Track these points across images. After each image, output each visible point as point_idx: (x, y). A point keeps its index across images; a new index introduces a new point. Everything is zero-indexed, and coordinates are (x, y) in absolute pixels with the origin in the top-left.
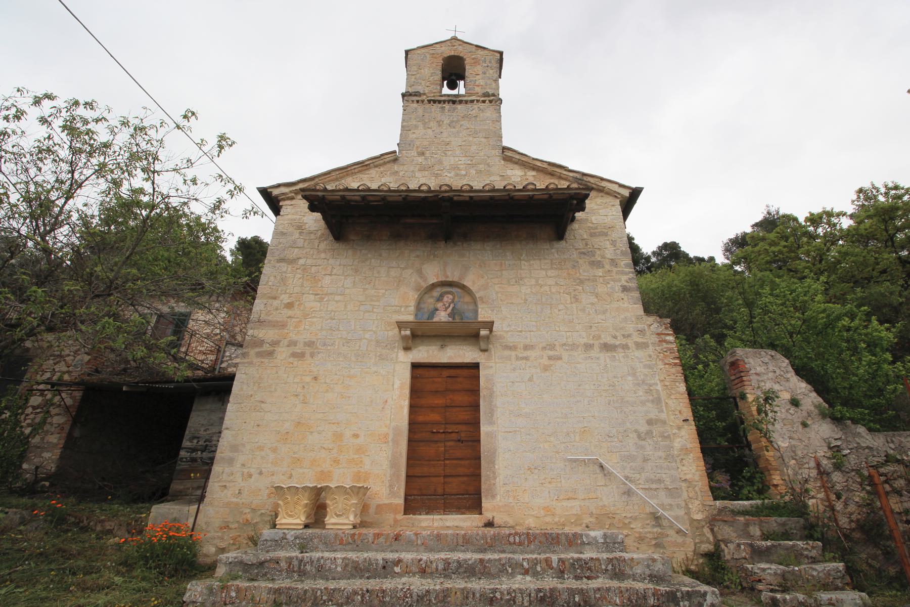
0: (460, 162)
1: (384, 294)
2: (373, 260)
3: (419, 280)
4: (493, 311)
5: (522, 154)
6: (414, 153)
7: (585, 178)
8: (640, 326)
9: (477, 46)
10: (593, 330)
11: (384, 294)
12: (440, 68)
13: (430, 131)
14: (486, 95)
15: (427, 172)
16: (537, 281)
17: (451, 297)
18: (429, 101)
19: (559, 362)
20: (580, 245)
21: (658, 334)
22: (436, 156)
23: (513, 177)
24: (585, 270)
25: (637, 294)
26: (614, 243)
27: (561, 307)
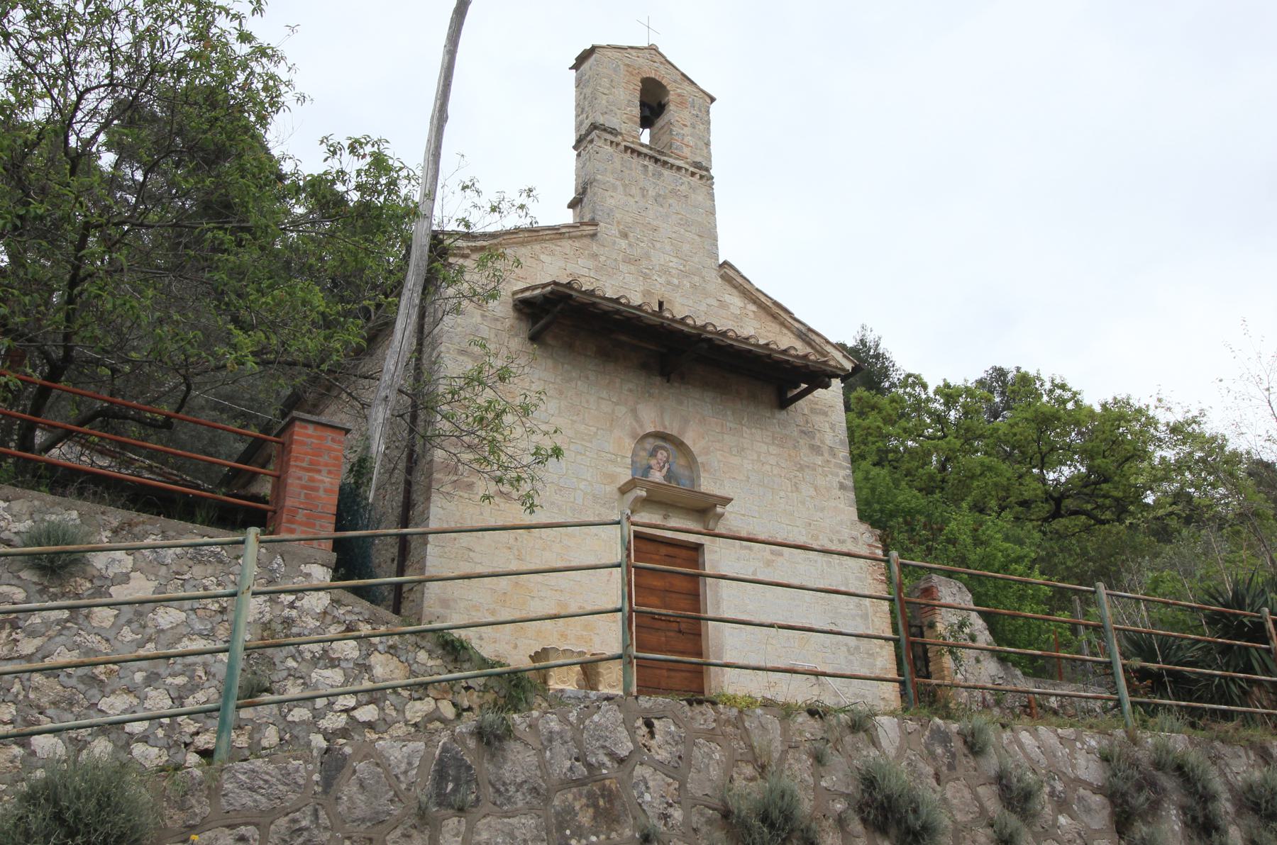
0: (671, 264)
1: (596, 433)
2: (579, 383)
3: (634, 423)
4: (715, 483)
5: (745, 278)
6: (614, 231)
7: (810, 334)
8: (854, 533)
9: (683, 75)
10: (812, 527)
11: (596, 433)
12: (638, 94)
13: (632, 201)
14: (698, 165)
15: (632, 267)
16: (759, 456)
17: (665, 454)
18: (626, 148)
19: (780, 559)
20: (800, 420)
21: (870, 545)
22: (642, 244)
23: (732, 307)
24: (806, 457)
25: (852, 495)
26: (833, 427)
27: (782, 494)
